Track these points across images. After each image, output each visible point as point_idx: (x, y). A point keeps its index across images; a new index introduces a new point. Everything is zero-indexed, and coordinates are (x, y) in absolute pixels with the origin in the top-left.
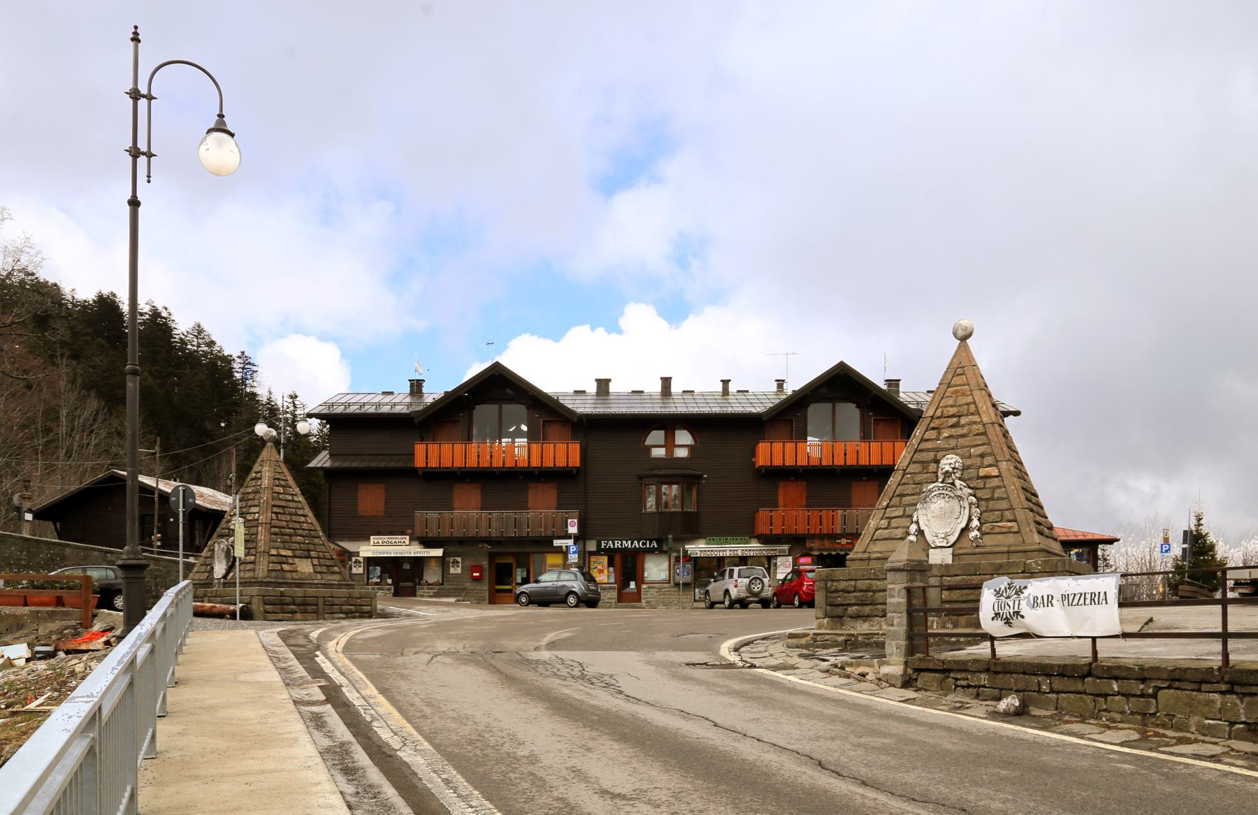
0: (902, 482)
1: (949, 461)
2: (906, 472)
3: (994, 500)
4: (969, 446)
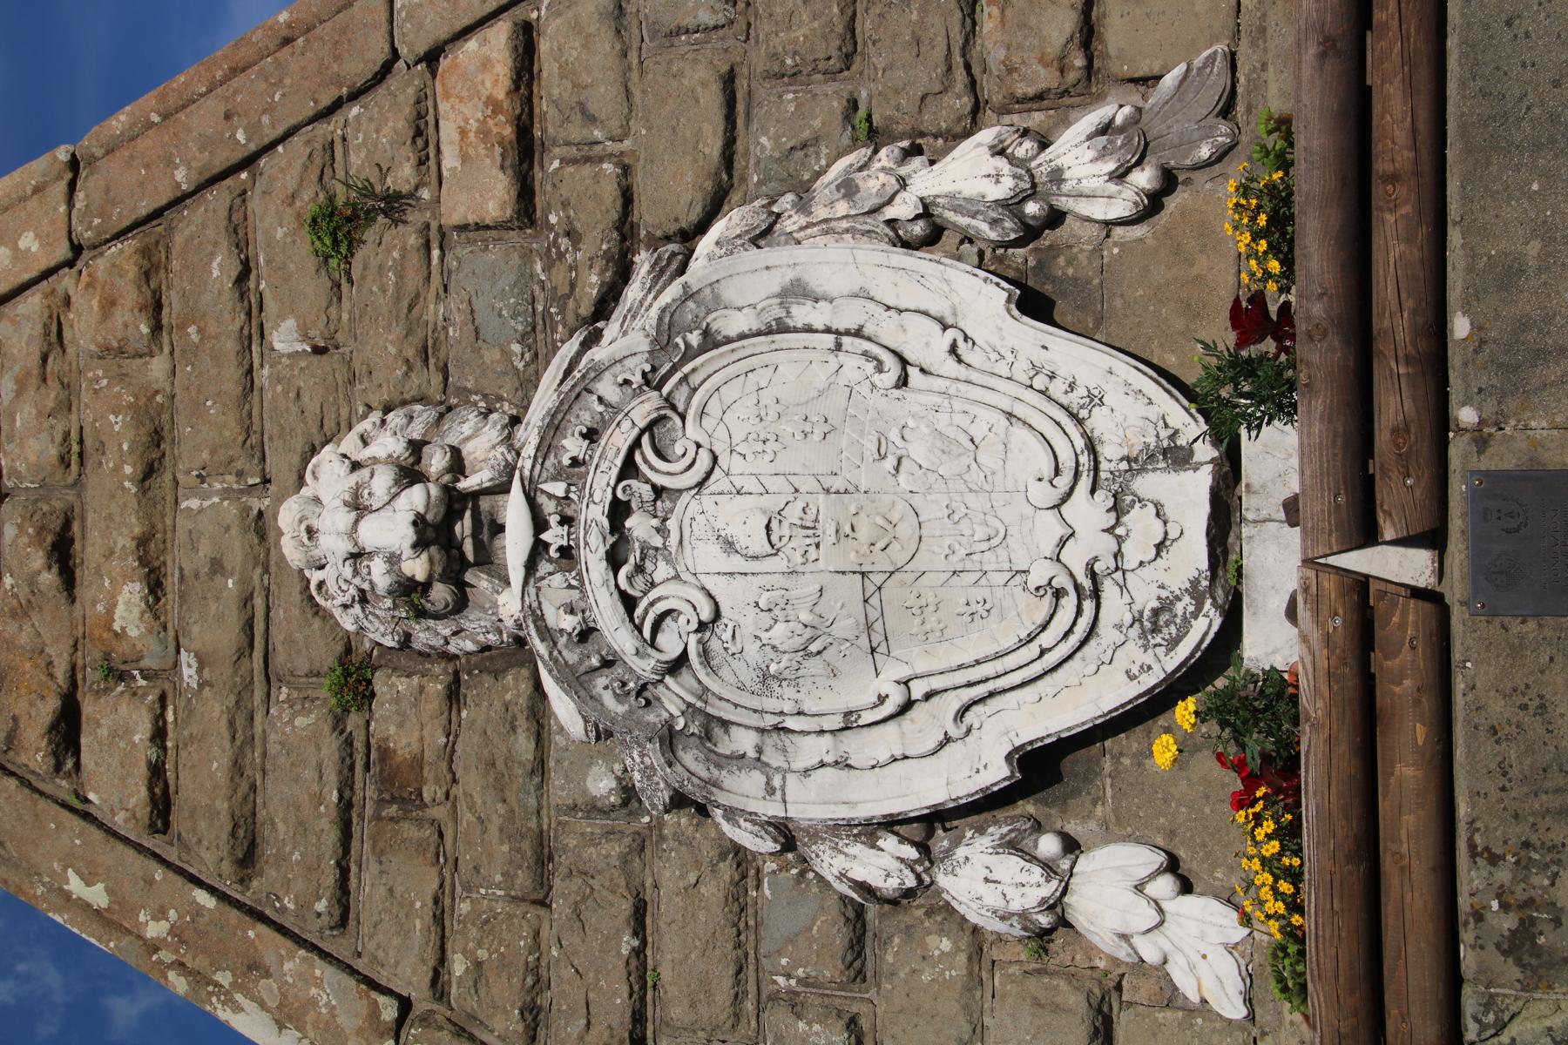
1: (334, 520)
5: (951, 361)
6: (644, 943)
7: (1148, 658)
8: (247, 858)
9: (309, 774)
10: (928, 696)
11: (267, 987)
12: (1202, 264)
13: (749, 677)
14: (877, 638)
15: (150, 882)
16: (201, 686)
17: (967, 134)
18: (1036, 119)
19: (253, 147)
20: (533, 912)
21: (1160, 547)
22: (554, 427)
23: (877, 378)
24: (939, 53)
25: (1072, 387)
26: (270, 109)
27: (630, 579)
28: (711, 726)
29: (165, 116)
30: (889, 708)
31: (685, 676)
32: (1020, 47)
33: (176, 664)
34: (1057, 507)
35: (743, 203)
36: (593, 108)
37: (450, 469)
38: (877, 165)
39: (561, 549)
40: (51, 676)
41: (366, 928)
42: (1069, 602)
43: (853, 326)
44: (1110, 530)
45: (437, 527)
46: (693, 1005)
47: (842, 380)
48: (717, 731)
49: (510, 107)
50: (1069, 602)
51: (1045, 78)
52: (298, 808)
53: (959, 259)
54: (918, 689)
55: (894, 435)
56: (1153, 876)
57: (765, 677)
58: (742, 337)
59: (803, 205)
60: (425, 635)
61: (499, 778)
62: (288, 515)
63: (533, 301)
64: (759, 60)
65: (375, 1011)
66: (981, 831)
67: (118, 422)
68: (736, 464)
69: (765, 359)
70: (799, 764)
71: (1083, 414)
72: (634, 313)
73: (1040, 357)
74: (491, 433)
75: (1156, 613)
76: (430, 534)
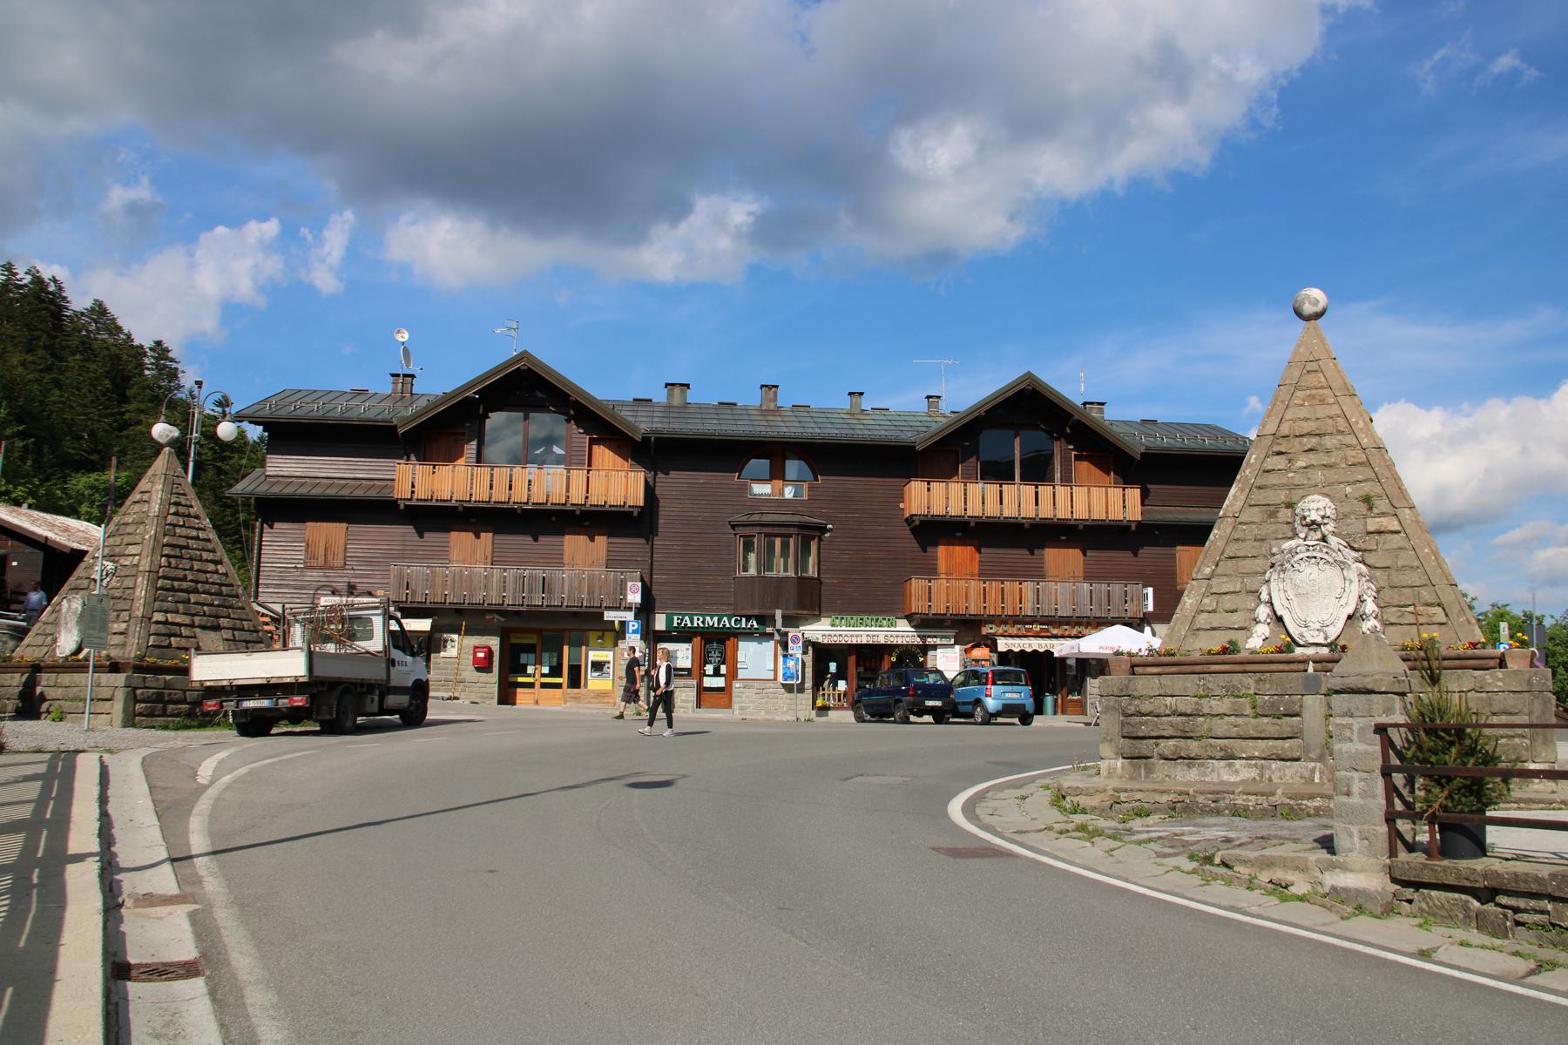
8: (1260, 488)
11: (1239, 493)
17: (1378, 606)
18: (1380, 617)
28: (1284, 571)
49: (1386, 530)
51: (1385, 618)
60: (1297, 518)
64: (1392, 572)
67: (1333, 460)
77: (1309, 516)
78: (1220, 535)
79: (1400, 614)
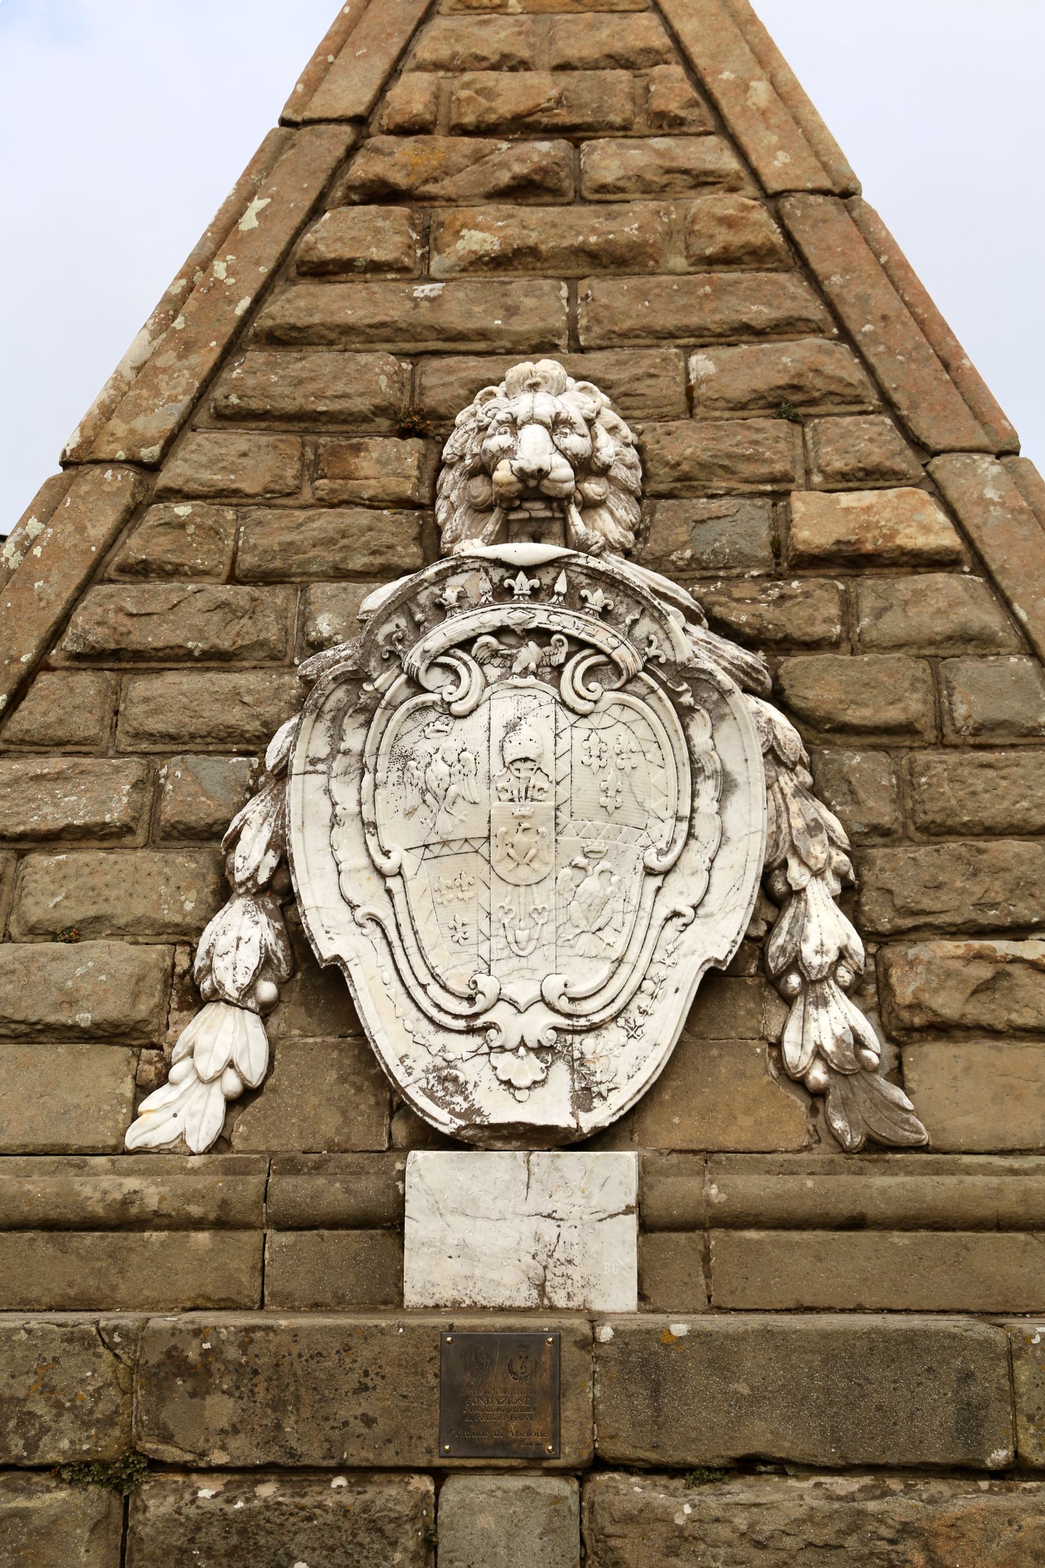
0: (117, 558)
1: (545, 405)
2: (164, 479)
3: (942, 744)
4: (671, 335)
5: (666, 912)
6: (197, 660)
7: (418, 1073)
9: (339, 387)
10: (389, 892)
11: (169, 358)
12: (747, 1121)
13: (406, 743)
14: (436, 850)
15: (258, 263)
16: (415, 300)
19: (859, 338)
20: (224, 570)
21: (508, 1083)
22: (612, 583)
23: (652, 850)
24: (927, 903)
25: (644, 1012)
26: (890, 352)
27: (487, 645)
29: (885, 267)
30: (380, 860)
31: (406, 692)
32: (929, 971)
33: (434, 280)
34: (543, 999)
35: (807, 743)
36: (888, 617)
37: (585, 497)
38: (834, 852)
39: (511, 588)
40: (426, 181)
41: (216, 435)
42: (465, 1009)
43: (697, 831)
44: (522, 1042)
45: (537, 488)
46: (146, 700)
47: (651, 822)
48: (361, 718)
50: (465, 1009)
52: (313, 379)
53: (754, 920)
54: (394, 883)
55: (605, 864)
56: (240, 1074)
57: (406, 757)
58: (688, 739)
59: (800, 791)
61: (332, 541)
62: (548, 367)
63: (726, 568)
65: (148, 443)
66: (279, 935)
68: (580, 733)
69: (670, 759)
70: (334, 785)
71: (621, 1021)
72: (713, 650)
73: (670, 986)
74: (617, 533)
75: (455, 1079)
76: (532, 483)
77: (508, 452)
78: (54, 550)
79: (984, 972)
